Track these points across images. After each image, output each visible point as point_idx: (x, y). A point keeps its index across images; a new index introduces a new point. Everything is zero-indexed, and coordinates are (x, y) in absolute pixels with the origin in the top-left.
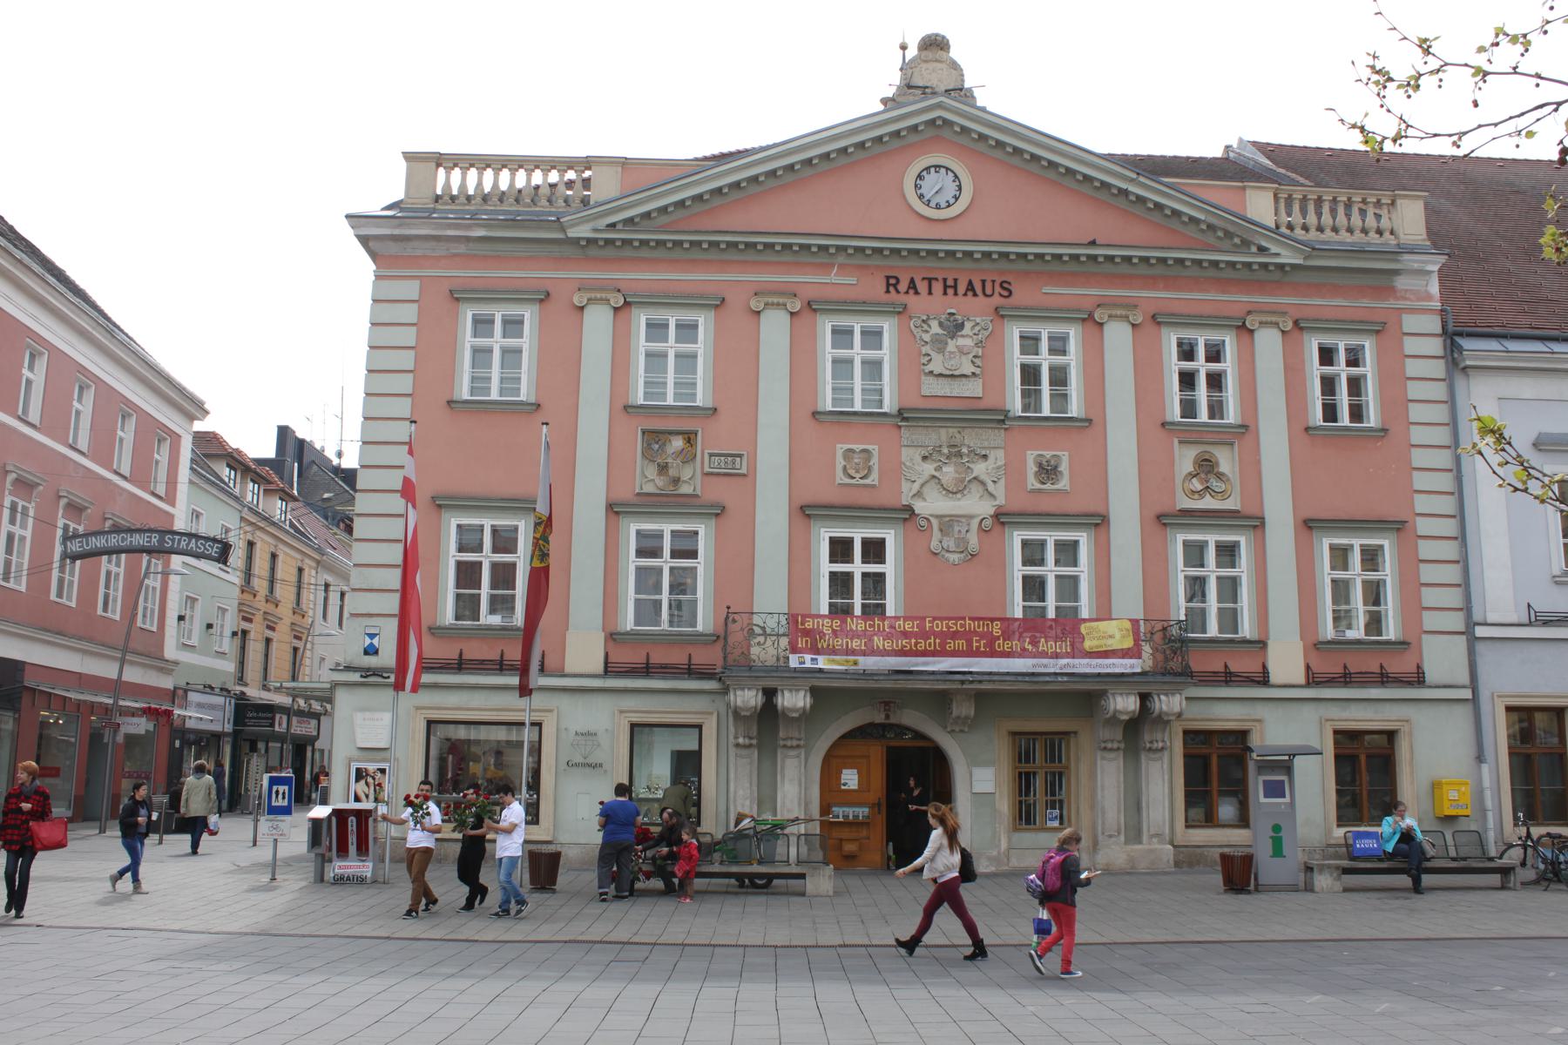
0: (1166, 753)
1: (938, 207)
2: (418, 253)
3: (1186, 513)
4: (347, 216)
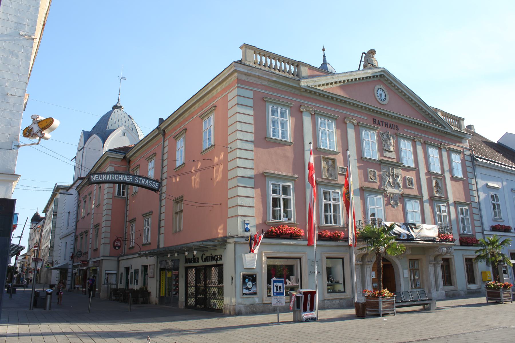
2: (251, 81)
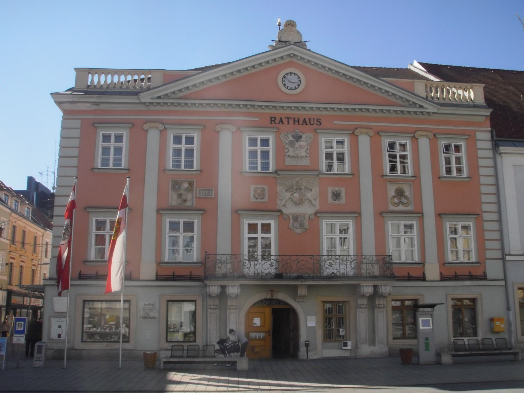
1: (291, 89)
4: (52, 94)
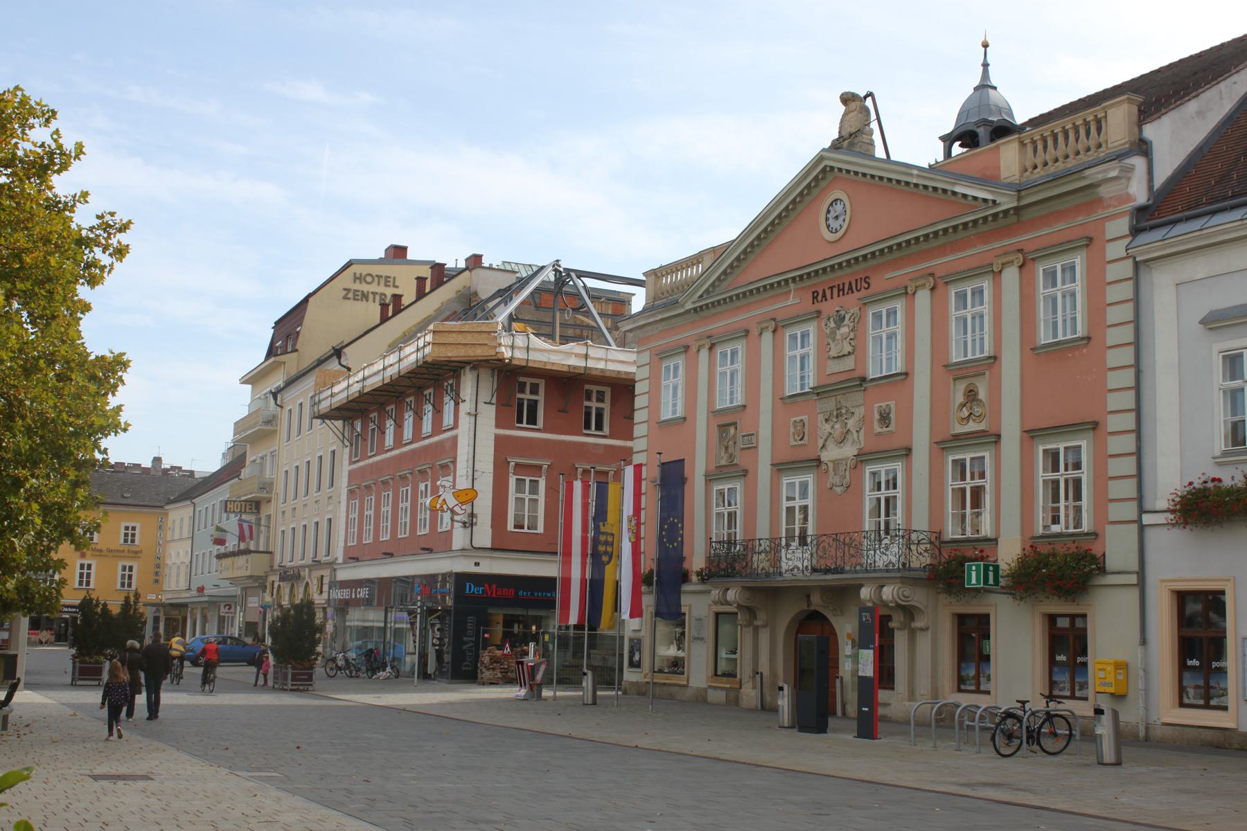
0: (929, 633)
3: (957, 437)
